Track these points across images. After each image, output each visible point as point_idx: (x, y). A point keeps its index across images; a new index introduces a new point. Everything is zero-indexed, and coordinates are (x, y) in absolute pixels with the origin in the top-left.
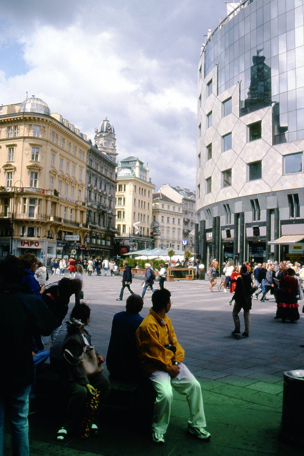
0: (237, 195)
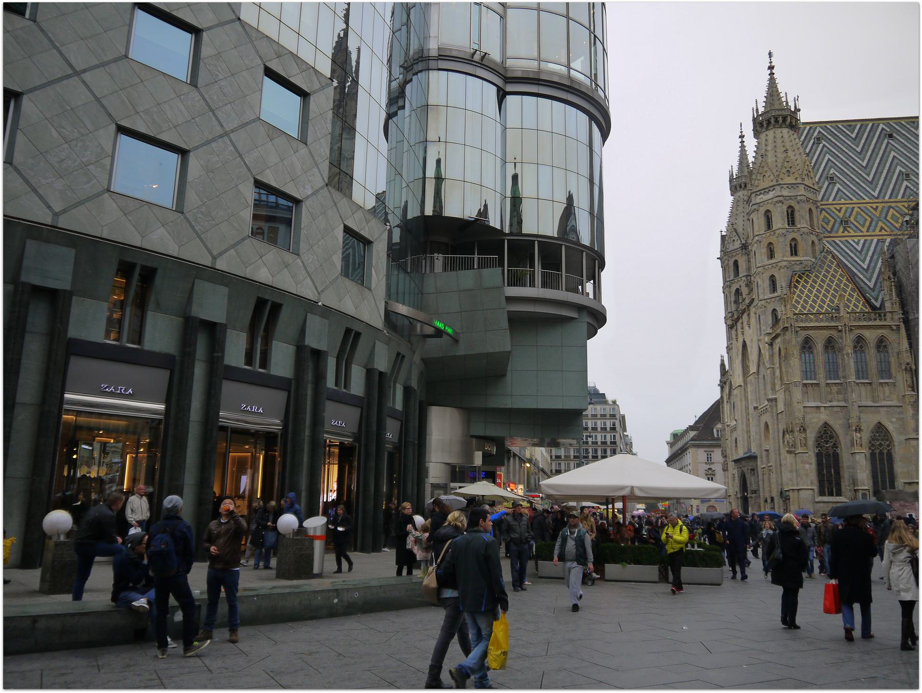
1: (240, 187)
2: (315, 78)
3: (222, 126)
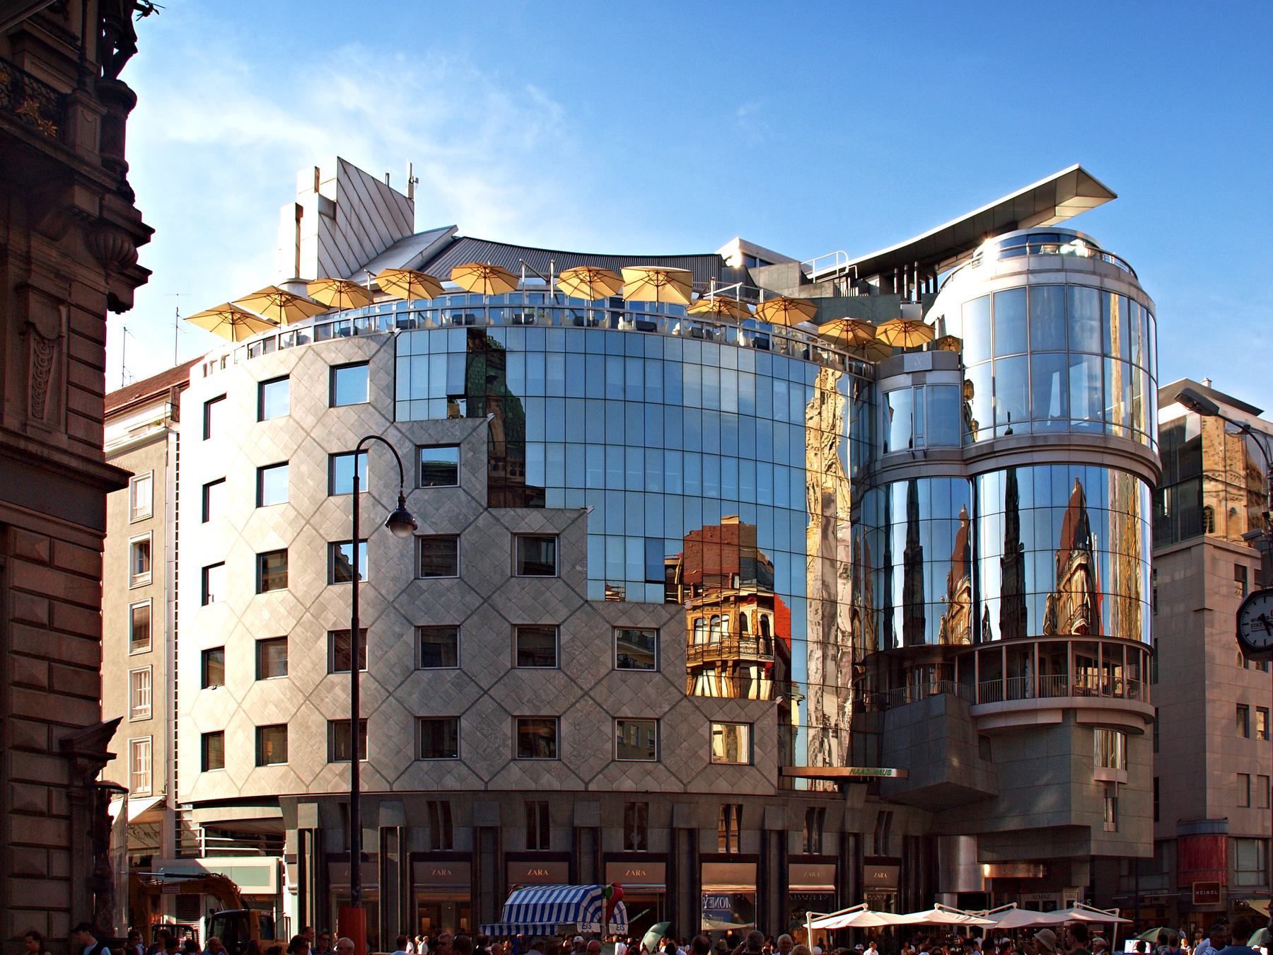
0: (584, 785)
1: (603, 728)
2: (663, 612)
3: (582, 689)
